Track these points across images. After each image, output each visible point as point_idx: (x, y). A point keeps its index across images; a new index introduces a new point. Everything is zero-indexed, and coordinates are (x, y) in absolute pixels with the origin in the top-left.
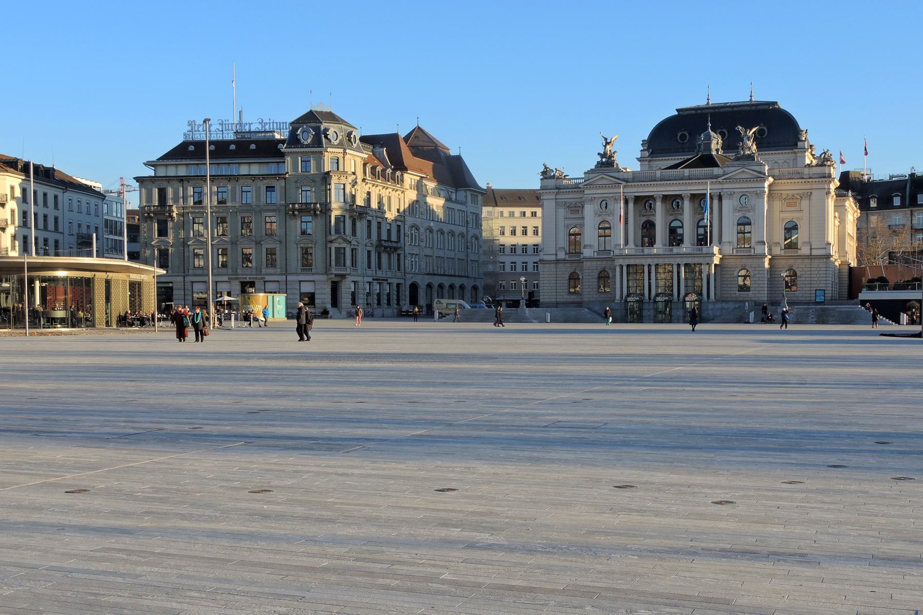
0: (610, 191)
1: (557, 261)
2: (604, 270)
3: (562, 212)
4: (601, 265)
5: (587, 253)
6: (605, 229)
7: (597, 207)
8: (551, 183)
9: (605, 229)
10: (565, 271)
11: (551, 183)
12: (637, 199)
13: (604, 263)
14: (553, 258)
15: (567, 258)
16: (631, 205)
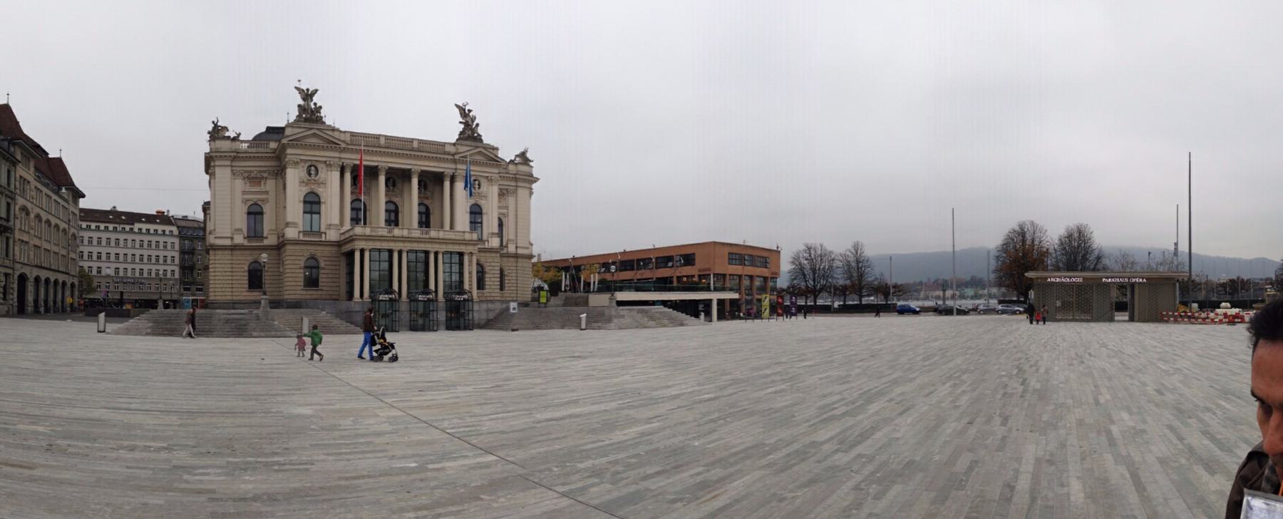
0: (323, 153)
1: (234, 248)
2: (313, 258)
3: (239, 184)
4: (308, 251)
5: (291, 233)
6: (312, 204)
7: (304, 174)
8: (224, 145)
9: (312, 204)
10: (243, 263)
11: (224, 145)
12: (355, 170)
13: (313, 248)
14: (228, 242)
15: (246, 243)
16: (348, 176)
